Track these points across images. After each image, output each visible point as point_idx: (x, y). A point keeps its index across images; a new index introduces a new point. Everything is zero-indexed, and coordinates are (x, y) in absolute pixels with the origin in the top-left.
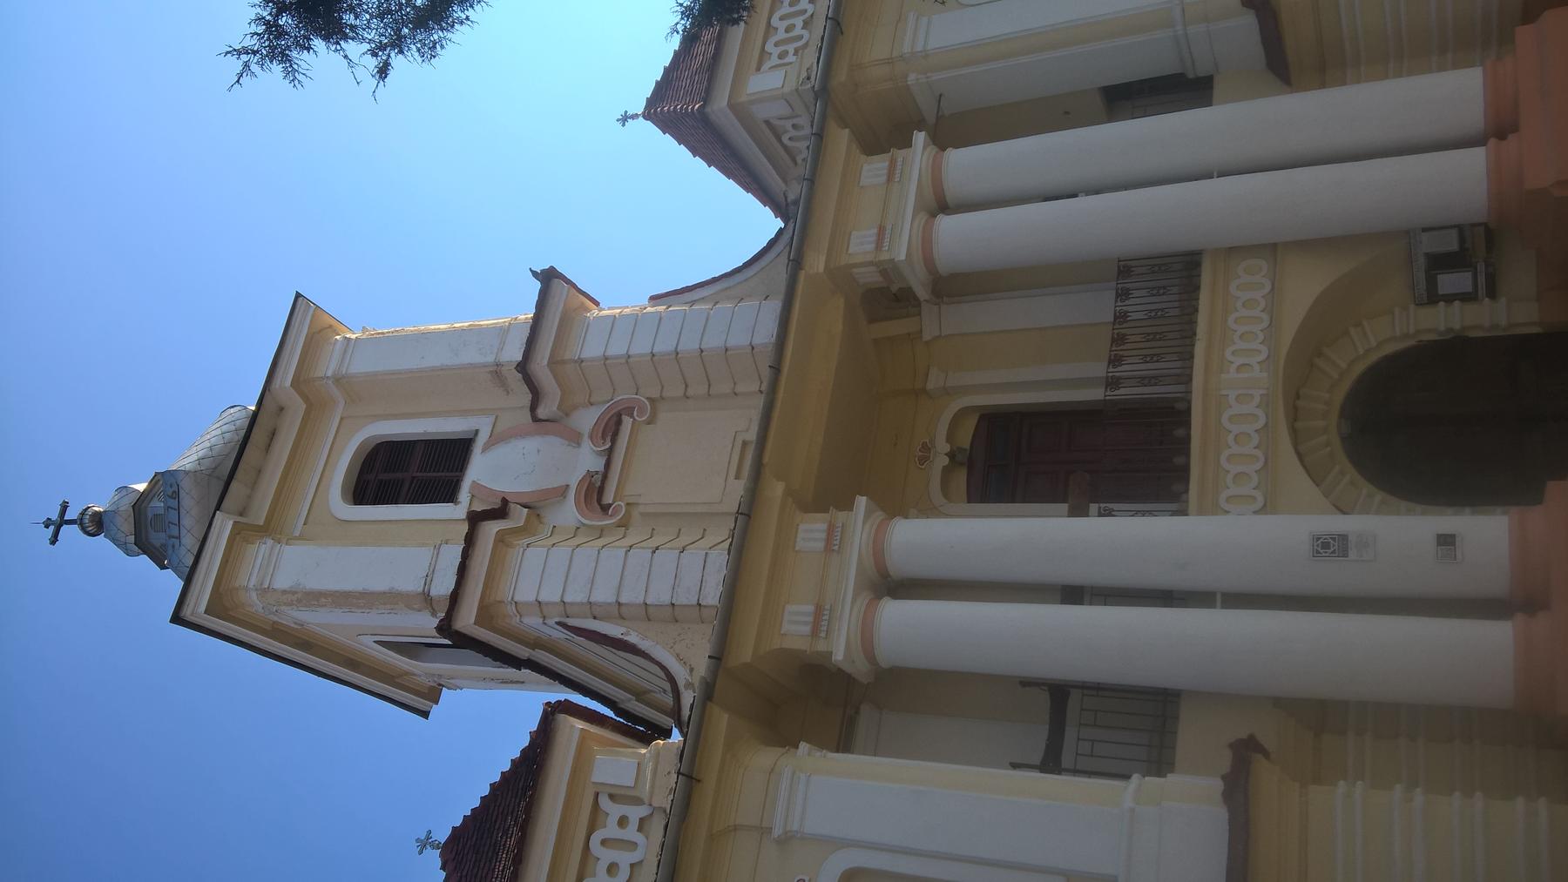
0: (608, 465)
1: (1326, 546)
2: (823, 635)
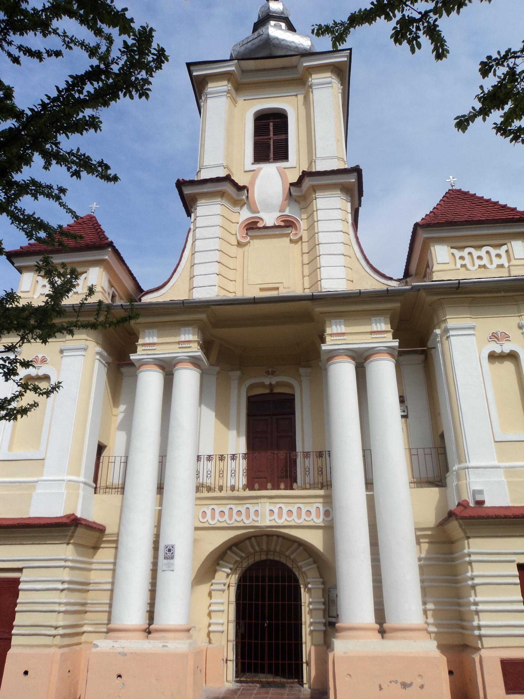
0: (265, 228)
1: (169, 550)
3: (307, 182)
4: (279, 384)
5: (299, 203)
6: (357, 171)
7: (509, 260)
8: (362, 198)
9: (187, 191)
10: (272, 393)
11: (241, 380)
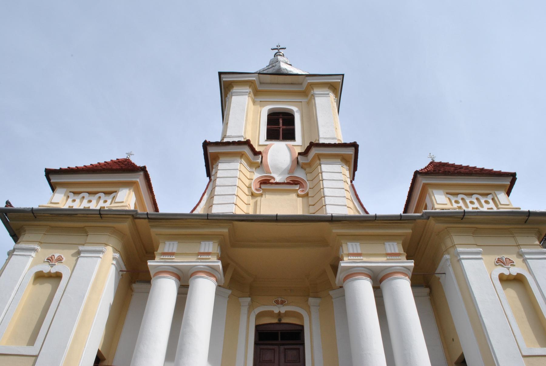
0: (277, 183)
2: (162, 257)
3: (314, 151)
4: (288, 314)
5: (305, 170)
6: (355, 146)
7: (496, 205)
8: (356, 172)
9: (211, 150)
10: (280, 323)
11: (251, 307)
